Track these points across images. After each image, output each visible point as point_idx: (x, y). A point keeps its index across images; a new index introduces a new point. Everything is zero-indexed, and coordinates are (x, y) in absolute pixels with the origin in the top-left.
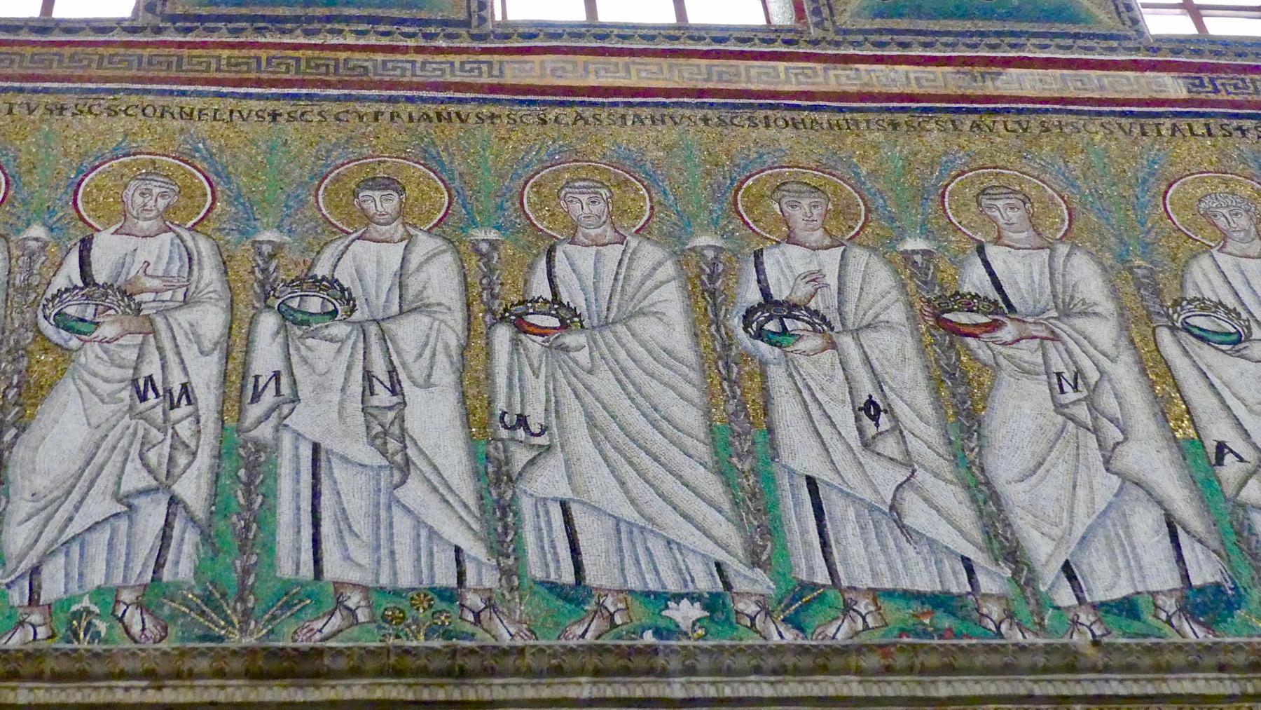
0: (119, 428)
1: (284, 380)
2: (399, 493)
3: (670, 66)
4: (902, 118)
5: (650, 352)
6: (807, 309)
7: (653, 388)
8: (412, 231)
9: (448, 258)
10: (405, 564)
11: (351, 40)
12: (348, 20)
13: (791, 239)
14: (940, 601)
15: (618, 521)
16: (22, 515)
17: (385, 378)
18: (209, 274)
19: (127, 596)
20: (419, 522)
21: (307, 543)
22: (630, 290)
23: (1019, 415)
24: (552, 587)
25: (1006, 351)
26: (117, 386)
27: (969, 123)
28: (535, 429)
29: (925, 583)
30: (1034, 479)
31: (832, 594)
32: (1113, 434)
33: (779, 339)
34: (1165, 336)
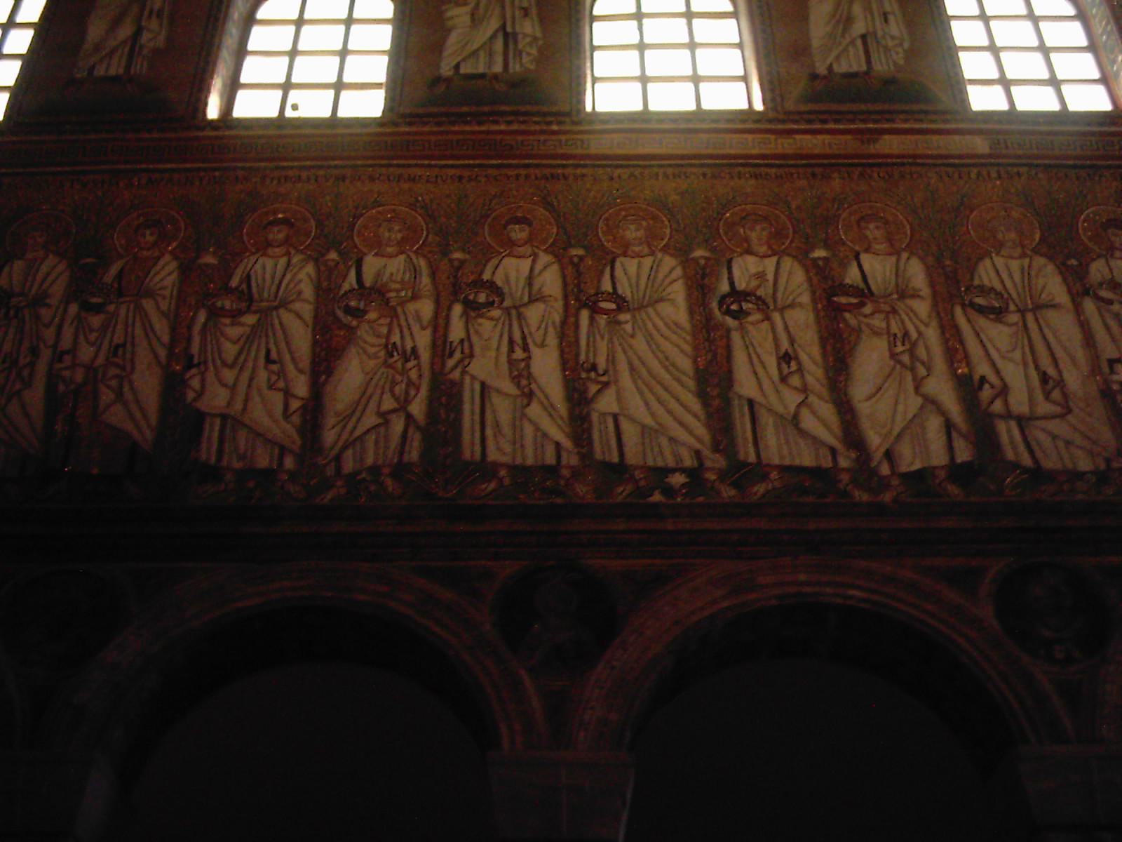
1: (466, 344)
4: (818, 170)
5: (666, 324)
6: (755, 296)
7: (667, 346)
8: (536, 250)
9: (555, 267)
10: (530, 451)
11: (503, 127)
12: (503, 114)
13: (749, 252)
14: (816, 472)
15: (644, 427)
16: (330, 426)
18: (425, 280)
20: (537, 429)
22: (656, 285)
23: (870, 360)
24: (608, 466)
25: (865, 320)
26: (376, 349)
27: (857, 173)
28: (601, 372)
29: (807, 460)
30: (874, 400)
32: (922, 371)
33: (739, 315)
34: (958, 311)
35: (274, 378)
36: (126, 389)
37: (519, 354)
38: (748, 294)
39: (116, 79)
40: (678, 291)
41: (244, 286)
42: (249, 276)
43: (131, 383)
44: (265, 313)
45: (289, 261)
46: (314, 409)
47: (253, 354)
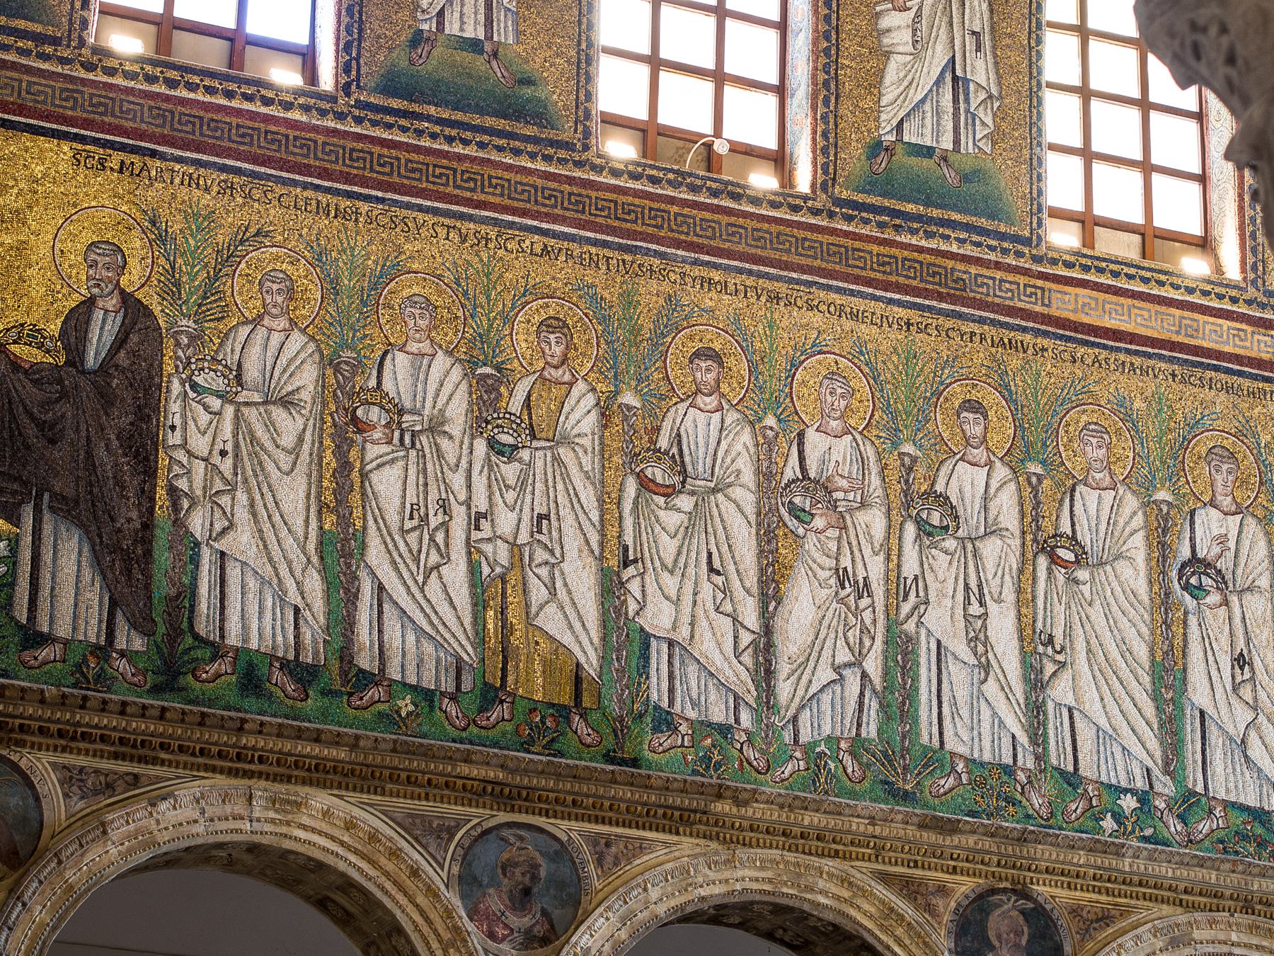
0: (831, 611)
2: (984, 687)
3: (1157, 312)
7: (1124, 623)
8: (993, 458)
9: (1012, 486)
11: (954, 248)
13: (1213, 503)
17: (976, 590)
18: (875, 481)
19: (843, 745)
20: (995, 714)
21: (935, 721)
22: (1116, 534)
24: (1062, 773)
28: (1058, 648)
29: (1252, 801)
31: (1204, 800)
33: (1197, 592)
35: (721, 596)
36: (559, 584)
37: (975, 609)
38: (1208, 565)
39: (475, 46)
40: (1137, 545)
41: (675, 450)
42: (679, 435)
43: (563, 573)
44: (701, 497)
45: (723, 421)
46: (765, 646)
47: (693, 555)
